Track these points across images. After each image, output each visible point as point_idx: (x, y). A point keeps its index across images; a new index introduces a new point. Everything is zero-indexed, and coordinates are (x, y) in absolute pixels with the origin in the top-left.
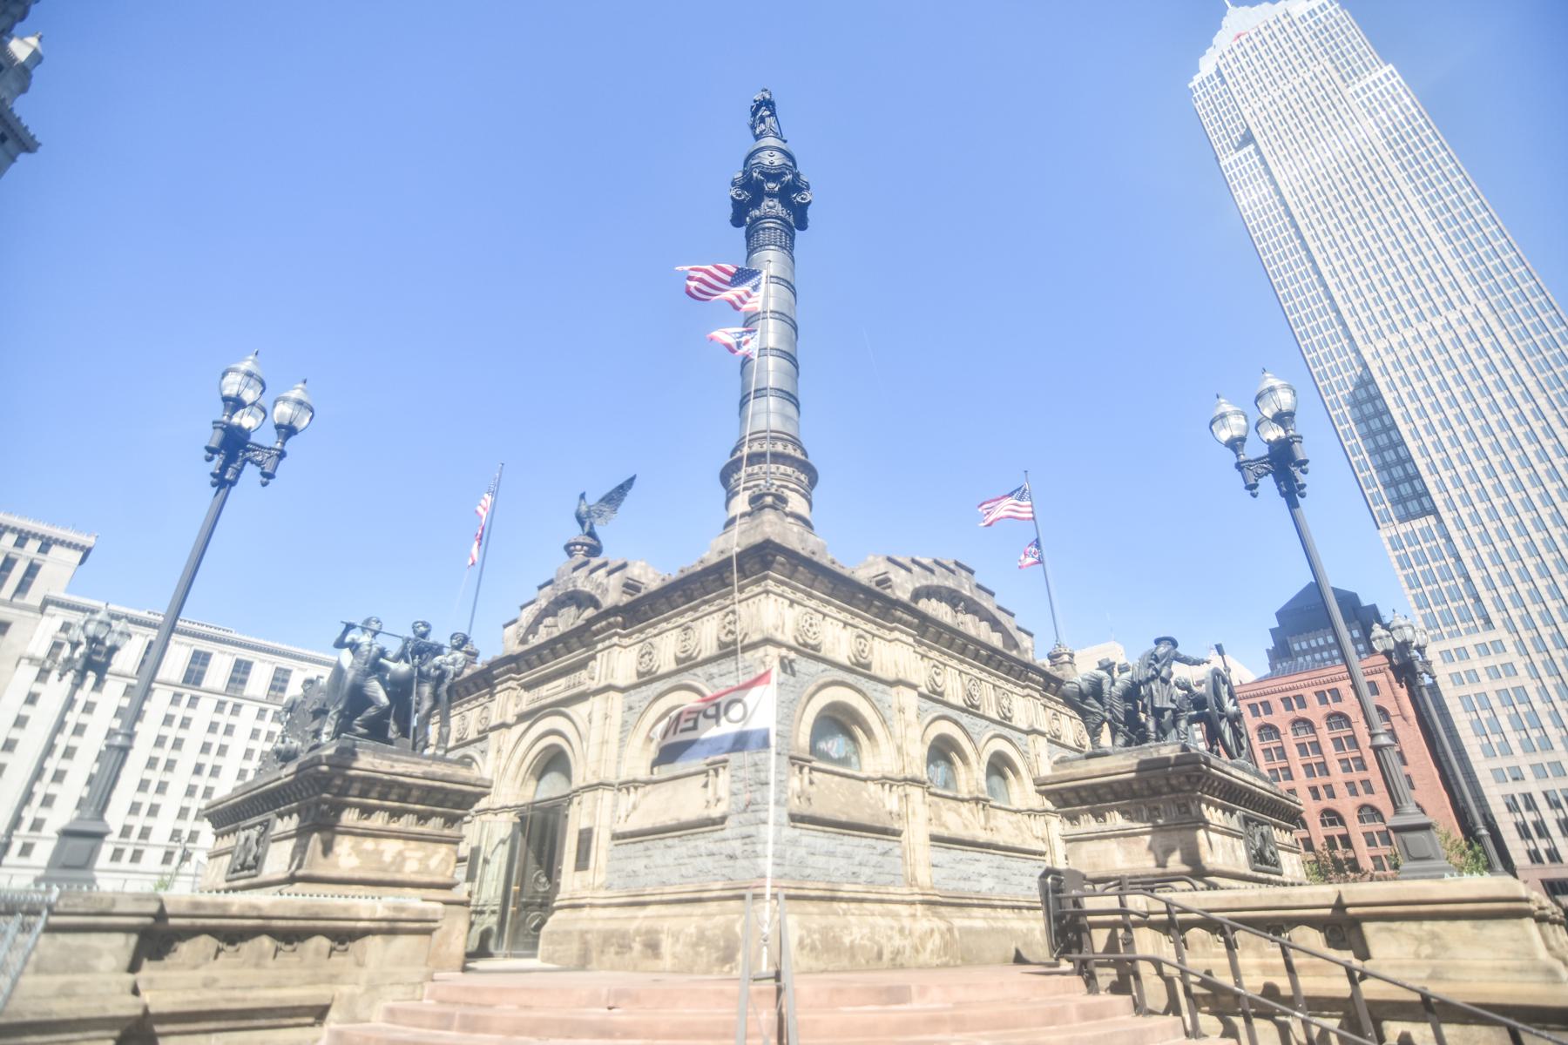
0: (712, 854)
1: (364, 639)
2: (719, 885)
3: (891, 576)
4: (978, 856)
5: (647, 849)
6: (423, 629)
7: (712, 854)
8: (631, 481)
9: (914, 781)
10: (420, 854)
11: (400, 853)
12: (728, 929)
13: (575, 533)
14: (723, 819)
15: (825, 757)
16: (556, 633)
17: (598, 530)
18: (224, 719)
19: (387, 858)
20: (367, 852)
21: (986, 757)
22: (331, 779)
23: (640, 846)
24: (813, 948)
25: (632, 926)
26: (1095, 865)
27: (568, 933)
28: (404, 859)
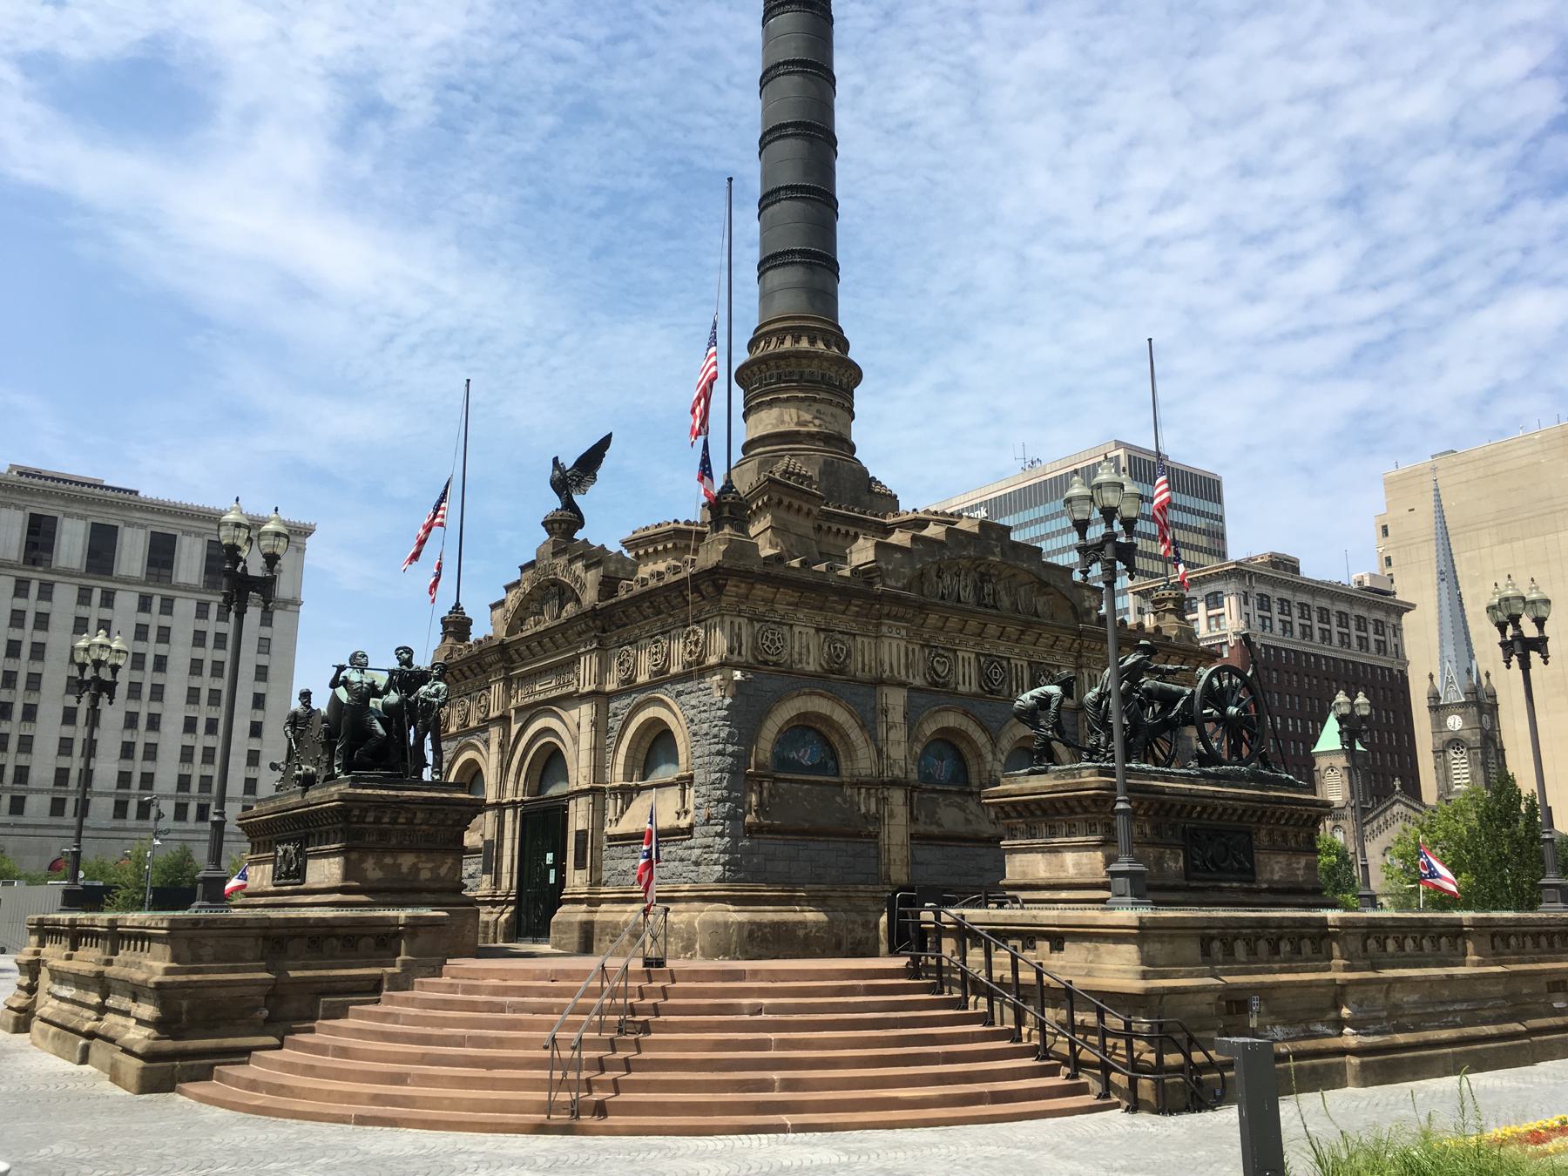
0: (682, 860)
1: (354, 676)
2: (687, 887)
4: (984, 851)
6: (406, 656)
7: (682, 860)
8: (605, 442)
9: (895, 783)
10: (430, 865)
12: (690, 924)
13: (554, 503)
14: (691, 827)
15: (796, 767)
16: (541, 628)
17: (577, 498)
18: (154, 619)
19: (405, 869)
21: (1006, 744)
22: (351, 810)
23: (627, 849)
24: (764, 939)
25: (623, 918)
26: (1024, 873)
27: (570, 924)
28: (418, 870)
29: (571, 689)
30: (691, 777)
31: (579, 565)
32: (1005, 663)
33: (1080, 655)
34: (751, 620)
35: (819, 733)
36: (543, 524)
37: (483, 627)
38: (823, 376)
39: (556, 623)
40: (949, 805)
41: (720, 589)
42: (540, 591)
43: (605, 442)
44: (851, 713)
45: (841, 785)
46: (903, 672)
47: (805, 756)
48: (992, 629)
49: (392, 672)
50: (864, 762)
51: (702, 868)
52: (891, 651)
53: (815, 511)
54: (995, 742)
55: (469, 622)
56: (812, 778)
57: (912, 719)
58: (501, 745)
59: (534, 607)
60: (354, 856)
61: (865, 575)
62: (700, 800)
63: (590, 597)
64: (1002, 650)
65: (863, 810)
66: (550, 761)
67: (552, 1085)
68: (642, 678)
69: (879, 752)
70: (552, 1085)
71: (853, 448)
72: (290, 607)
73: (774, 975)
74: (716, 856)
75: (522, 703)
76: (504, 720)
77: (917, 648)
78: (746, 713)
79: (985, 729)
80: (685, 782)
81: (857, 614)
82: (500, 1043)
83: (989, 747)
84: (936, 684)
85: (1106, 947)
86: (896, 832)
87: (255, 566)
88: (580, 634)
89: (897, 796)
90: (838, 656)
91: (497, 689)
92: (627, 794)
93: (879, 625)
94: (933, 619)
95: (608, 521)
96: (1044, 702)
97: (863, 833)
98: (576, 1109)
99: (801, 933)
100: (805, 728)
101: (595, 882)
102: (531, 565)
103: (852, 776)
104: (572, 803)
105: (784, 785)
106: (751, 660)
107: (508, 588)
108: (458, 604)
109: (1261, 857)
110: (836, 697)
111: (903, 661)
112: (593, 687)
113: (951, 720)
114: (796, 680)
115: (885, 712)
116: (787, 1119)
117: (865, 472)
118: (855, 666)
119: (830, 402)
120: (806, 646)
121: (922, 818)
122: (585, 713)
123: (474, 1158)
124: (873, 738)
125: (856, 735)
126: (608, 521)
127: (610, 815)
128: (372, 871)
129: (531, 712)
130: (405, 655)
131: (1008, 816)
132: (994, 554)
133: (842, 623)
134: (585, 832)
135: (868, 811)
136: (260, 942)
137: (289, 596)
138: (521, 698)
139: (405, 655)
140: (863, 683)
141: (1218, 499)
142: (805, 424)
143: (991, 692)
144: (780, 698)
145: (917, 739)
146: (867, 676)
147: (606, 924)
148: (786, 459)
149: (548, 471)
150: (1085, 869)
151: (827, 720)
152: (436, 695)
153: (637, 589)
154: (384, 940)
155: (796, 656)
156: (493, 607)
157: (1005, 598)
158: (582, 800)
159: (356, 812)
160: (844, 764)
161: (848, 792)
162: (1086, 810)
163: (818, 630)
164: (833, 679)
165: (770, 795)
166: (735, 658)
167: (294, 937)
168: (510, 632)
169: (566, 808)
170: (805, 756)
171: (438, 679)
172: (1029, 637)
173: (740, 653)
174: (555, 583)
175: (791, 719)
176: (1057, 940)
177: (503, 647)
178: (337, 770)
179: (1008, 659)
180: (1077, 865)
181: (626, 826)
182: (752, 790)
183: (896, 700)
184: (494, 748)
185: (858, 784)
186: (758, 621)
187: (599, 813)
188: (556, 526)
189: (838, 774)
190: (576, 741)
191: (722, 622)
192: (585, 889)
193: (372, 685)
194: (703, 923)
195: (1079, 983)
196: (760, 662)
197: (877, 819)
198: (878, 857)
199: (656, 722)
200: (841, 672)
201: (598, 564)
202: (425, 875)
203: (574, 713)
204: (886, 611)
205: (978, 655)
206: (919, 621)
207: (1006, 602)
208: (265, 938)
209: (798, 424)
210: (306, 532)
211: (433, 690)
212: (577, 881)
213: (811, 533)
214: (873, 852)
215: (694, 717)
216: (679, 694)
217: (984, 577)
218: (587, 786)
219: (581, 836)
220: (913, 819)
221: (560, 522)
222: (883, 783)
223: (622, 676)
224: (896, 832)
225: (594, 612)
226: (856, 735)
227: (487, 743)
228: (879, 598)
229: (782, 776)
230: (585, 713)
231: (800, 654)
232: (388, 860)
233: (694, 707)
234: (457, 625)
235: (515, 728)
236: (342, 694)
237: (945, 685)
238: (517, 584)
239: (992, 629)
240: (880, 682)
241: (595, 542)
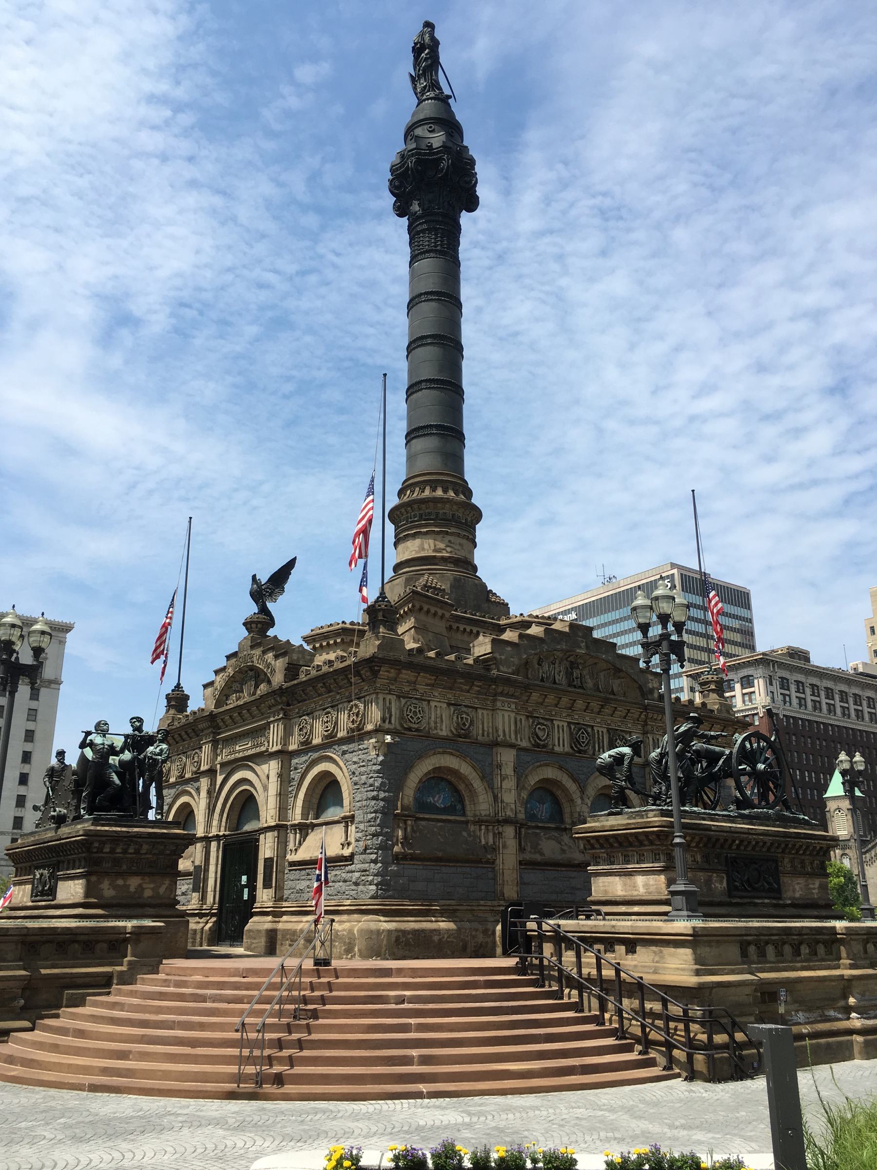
0: (345, 881)
1: (98, 740)
2: (348, 902)
4: (574, 874)
5: (308, 875)
6: (138, 724)
7: (345, 881)
8: (291, 564)
9: (507, 821)
10: (152, 886)
11: (140, 885)
12: (351, 931)
13: (253, 608)
14: (351, 858)
16: (240, 703)
17: (270, 605)
19: (132, 889)
20: (119, 885)
21: (591, 792)
22: (92, 843)
23: (303, 872)
24: (407, 944)
25: (300, 926)
26: (606, 892)
27: (259, 931)
29: (263, 749)
30: (353, 817)
31: (270, 656)
32: (589, 730)
33: (645, 724)
34: (399, 697)
35: (450, 783)
36: (244, 624)
37: (197, 702)
38: (453, 515)
39: (253, 698)
40: (548, 839)
41: (375, 674)
42: (241, 673)
43: (291, 564)
44: (473, 767)
45: (467, 822)
46: (513, 736)
47: (439, 800)
48: (580, 704)
49: (127, 737)
51: (361, 888)
52: (503, 720)
53: (447, 615)
54: (583, 790)
55: (187, 697)
56: (444, 817)
57: (520, 772)
58: (209, 792)
59: (236, 686)
60: (94, 879)
61: (483, 662)
62: (360, 835)
63: (278, 679)
64: (587, 719)
65: (483, 842)
66: (246, 805)
67: (241, 1061)
68: (317, 741)
69: (495, 798)
70: (241, 1061)
71: (475, 569)
72: (53, 686)
73: (414, 972)
74: (371, 878)
75: (225, 759)
76: (211, 773)
77: (524, 718)
78: (394, 767)
79: (575, 780)
81: (479, 693)
82: (202, 1026)
83: (579, 794)
84: (538, 746)
85: (669, 951)
86: (508, 859)
87: (26, 657)
88: (270, 707)
89: (509, 831)
90: (464, 724)
91: (207, 749)
92: (304, 829)
93: (494, 701)
94: (535, 696)
95: (292, 623)
96: (619, 759)
97: (482, 860)
98: (260, 1079)
99: (436, 938)
100: (439, 779)
101: (279, 898)
102: (234, 655)
103: (475, 816)
104: (262, 837)
105: (423, 823)
106: (399, 727)
107: (217, 672)
108: (179, 684)
109: (785, 880)
110: (463, 756)
111: (513, 728)
112: (279, 747)
113: (550, 773)
114: (432, 742)
115: (499, 767)
116: (423, 1087)
117: (484, 586)
118: (477, 731)
119: (459, 535)
120: (439, 716)
121: (528, 848)
122: (272, 767)
123: (180, 1119)
124: (491, 786)
125: (477, 784)
126: (292, 623)
127: (291, 846)
128: (107, 890)
129: (232, 766)
130: (137, 722)
131: (593, 848)
132: (580, 648)
133: (467, 699)
134: (271, 859)
135: (487, 843)
136: (19, 946)
137: (53, 678)
138: (225, 756)
139: (137, 722)
140: (482, 745)
141: (748, 607)
143: (580, 752)
144: (421, 757)
145: (524, 788)
146: (485, 739)
147: (286, 932)
148: (426, 577)
149: (248, 585)
150: (652, 889)
151: (455, 773)
152: (160, 754)
153: (314, 673)
154: (113, 945)
155: (433, 725)
156: (205, 686)
157: (589, 681)
158: (270, 835)
159: (96, 845)
160: (468, 808)
161: (472, 828)
162: (652, 843)
163: (449, 704)
164: (461, 741)
165: (413, 831)
166: (387, 725)
167: (45, 942)
169: (258, 840)
170: (439, 800)
171: (162, 741)
172: (607, 710)
173: (390, 722)
174: (252, 668)
175: (429, 773)
176: (631, 944)
177: (212, 716)
179: (592, 727)
180: (646, 885)
181: (303, 854)
182: (399, 827)
183: (507, 757)
184: (204, 793)
185: (479, 822)
186: (404, 698)
187: (282, 844)
188: (254, 626)
189: (464, 815)
190: (266, 788)
191: (377, 698)
192: (270, 904)
193: (112, 747)
194: (361, 931)
195: (649, 978)
196: (405, 729)
197: (494, 849)
198: (494, 879)
199: (326, 774)
200: (466, 736)
201: (284, 654)
202: (148, 893)
203: (265, 767)
204: (500, 690)
205: (569, 723)
206: (525, 698)
207: (590, 683)
208: (23, 943)
209: (435, 550)
210: (66, 628)
211: (158, 750)
212: (265, 898)
213: (445, 633)
214: (490, 875)
215: (354, 772)
216: (344, 753)
217: (573, 665)
218: (273, 824)
219: (268, 861)
220: (521, 849)
221: (257, 623)
222: (498, 821)
223: (302, 739)
224: (508, 859)
225: (281, 691)
226: (477, 784)
227: (198, 790)
228: (495, 680)
229: (421, 816)
230: (272, 767)
231: (436, 723)
232: (120, 882)
233: (355, 763)
234: (177, 700)
235: (220, 779)
236: (89, 753)
237: (544, 746)
238: (223, 669)
239: (580, 704)
240: (496, 744)
241: (283, 638)
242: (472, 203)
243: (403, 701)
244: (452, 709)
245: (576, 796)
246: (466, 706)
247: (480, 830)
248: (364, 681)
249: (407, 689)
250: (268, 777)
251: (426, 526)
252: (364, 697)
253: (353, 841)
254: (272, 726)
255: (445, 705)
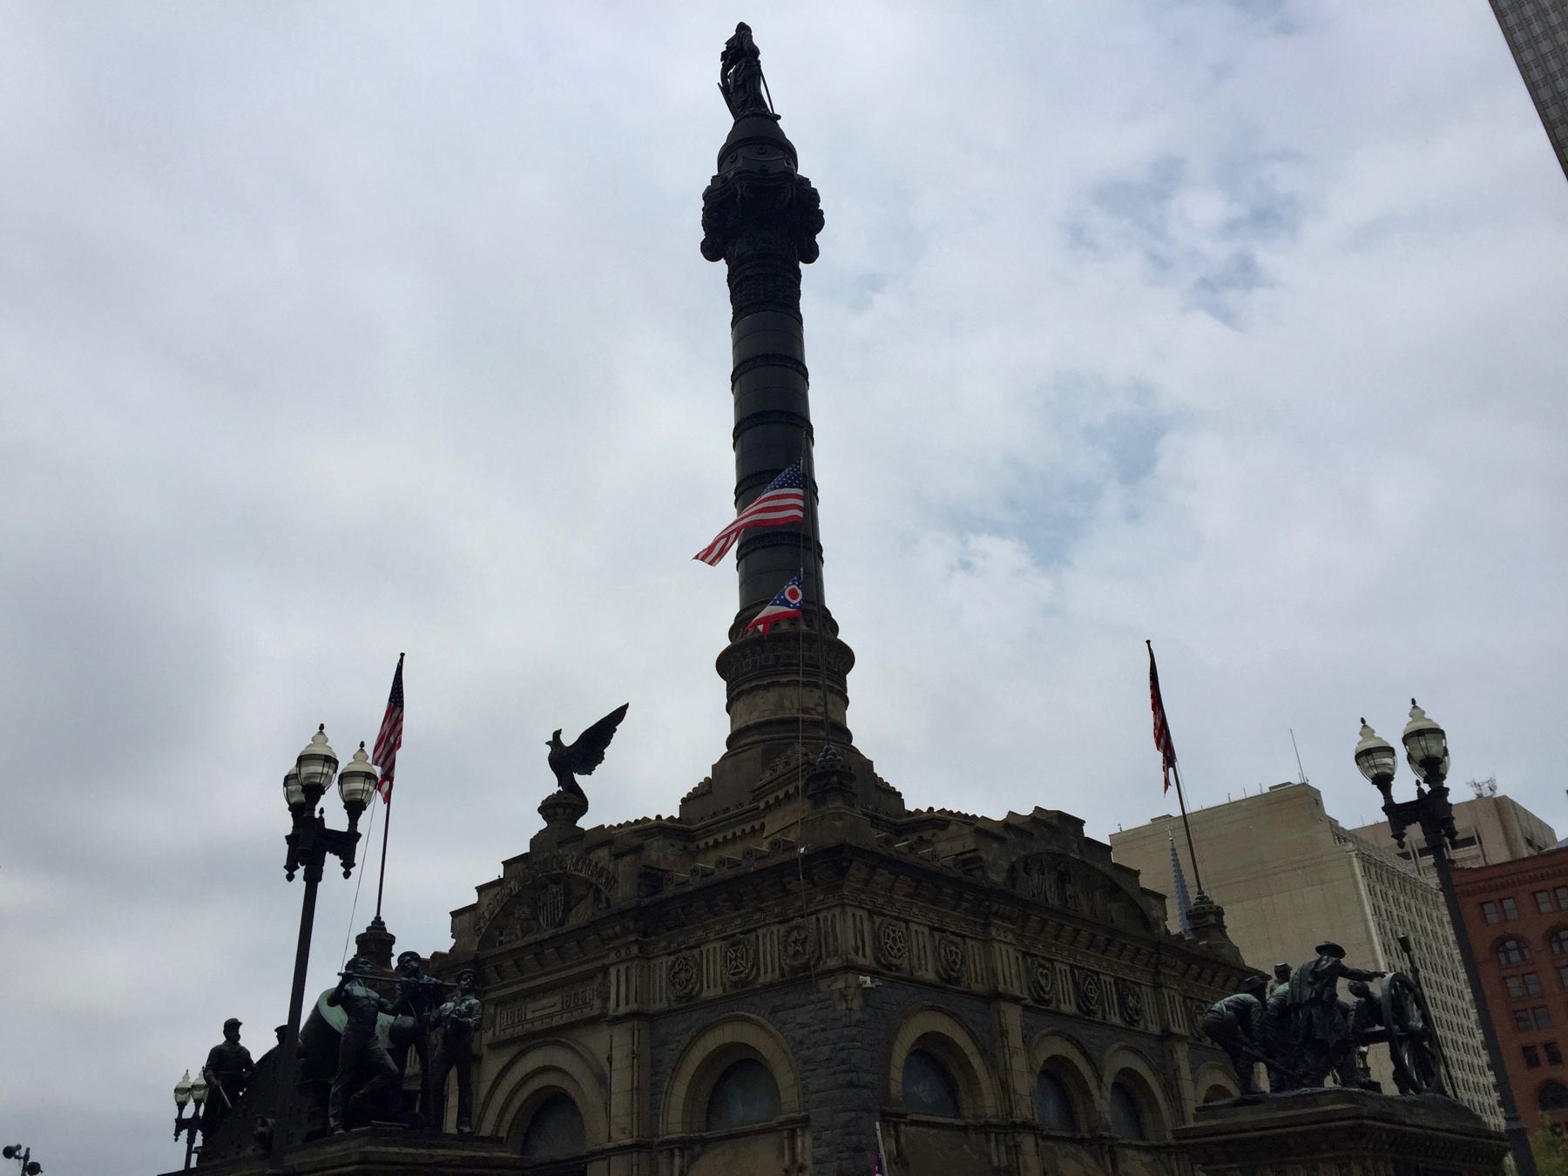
3: (982, 854)
8: (620, 714)
9: (1027, 1127)
13: (550, 785)
17: (578, 778)
21: (1109, 1079)
29: (588, 1012)
30: (806, 1120)
34: (871, 913)
36: (540, 810)
43: (620, 714)
45: (964, 1129)
48: (1084, 936)
50: (989, 1104)
54: (1099, 1078)
55: (391, 940)
65: (995, 1163)
68: (711, 993)
79: (1089, 1060)
80: (792, 1128)
84: (1041, 1000)
89: (1028, 1142)
93: (987, 926)
96: (1242, 1009)
108: (378, 918)
112: (633, 1007)
113: (1059, 1047)
115: (1004, 1034)
125: (976, 1061)
142: (806, 711)
163: (932, 929)
166: (860, 960)
168: (485, 941)
177: (477, 962)
178: (332, 1123)
183: (1012, 1017)
185: (985, 1128)
188: (559, 810)
190: (603, 1081)
191: (843, 913)
196: (885, 967)
204: (995, 906)
211: (463, 1007)
218: (628, 1142)
222: (1015, 1125)
226: (976, 1061)
233: (803, 1026)
238: (498, 882)
239: (1084, 936)
240: (994, 997)
242: (811, 254)
243: (878, 920)
244: (937, 935)
245: (1092, 1085)
246: (953, 933)
247: (988, 1141)
248: (815, 885)
249: (880, 901)
250: (610, 1060)
251: (784, 674)
252: (816, 912)
253: (809, 1163)
254: (613, 971)
255: (926, 931)
